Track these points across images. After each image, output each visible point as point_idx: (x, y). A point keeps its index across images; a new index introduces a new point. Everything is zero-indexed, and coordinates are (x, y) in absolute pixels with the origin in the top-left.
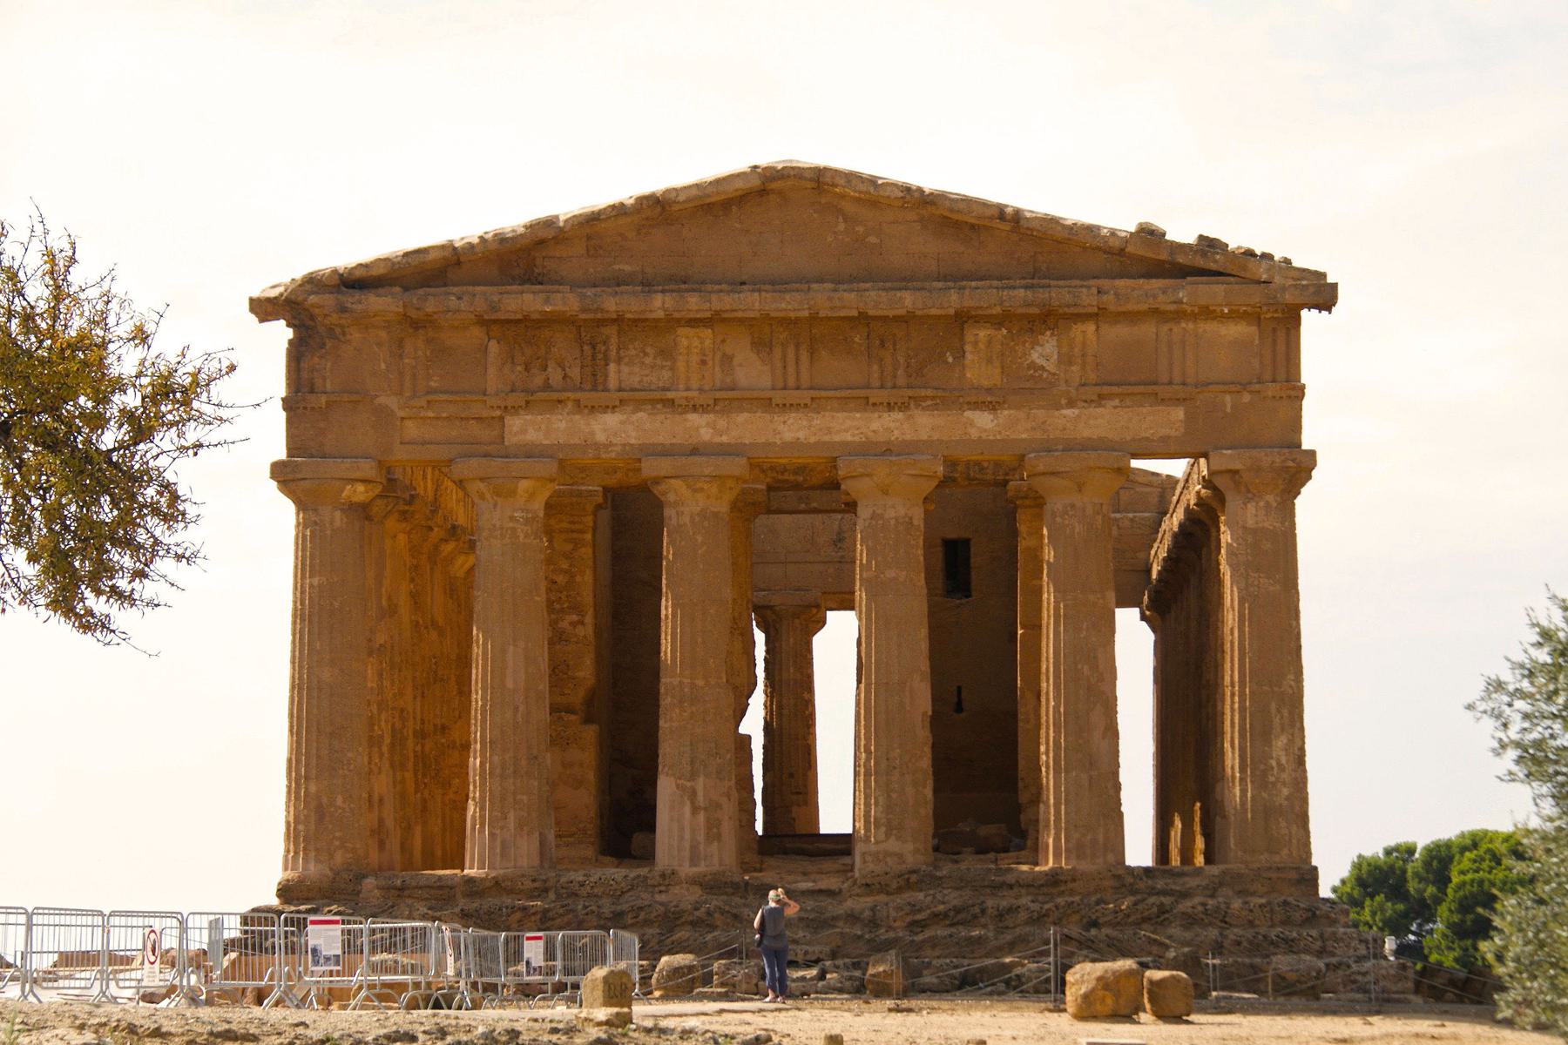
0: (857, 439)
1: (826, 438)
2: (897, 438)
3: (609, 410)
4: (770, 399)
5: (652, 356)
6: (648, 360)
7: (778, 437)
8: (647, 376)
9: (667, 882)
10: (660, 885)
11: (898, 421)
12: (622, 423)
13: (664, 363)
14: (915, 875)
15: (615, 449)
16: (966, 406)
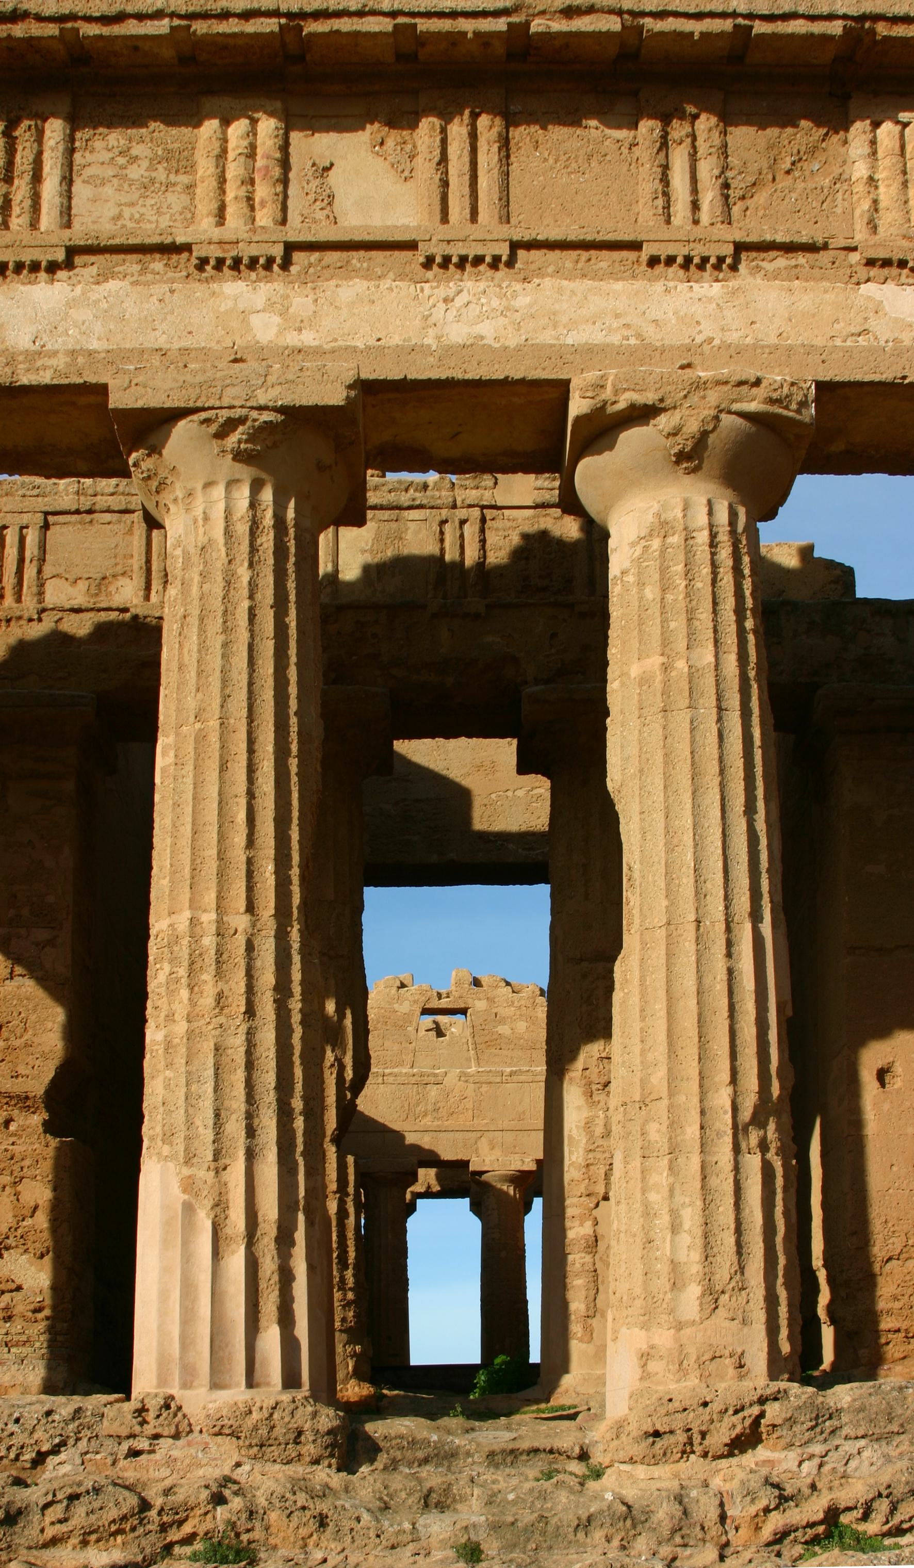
0: (615, 339)
1: (547, 337)
2: (710, 340)
3: (43, 275)
4: (412, 246)
5: (145, 164)
6: (136, 172)
7: (431, 332)
8: (132, 204)
9: (149, 1429)
10: (133, 1436)
11: (710, 300)
12: (71, 304)
13: (172, 178)
14: (777, 1405)
15: (53, 362)
16: (863, 272)
